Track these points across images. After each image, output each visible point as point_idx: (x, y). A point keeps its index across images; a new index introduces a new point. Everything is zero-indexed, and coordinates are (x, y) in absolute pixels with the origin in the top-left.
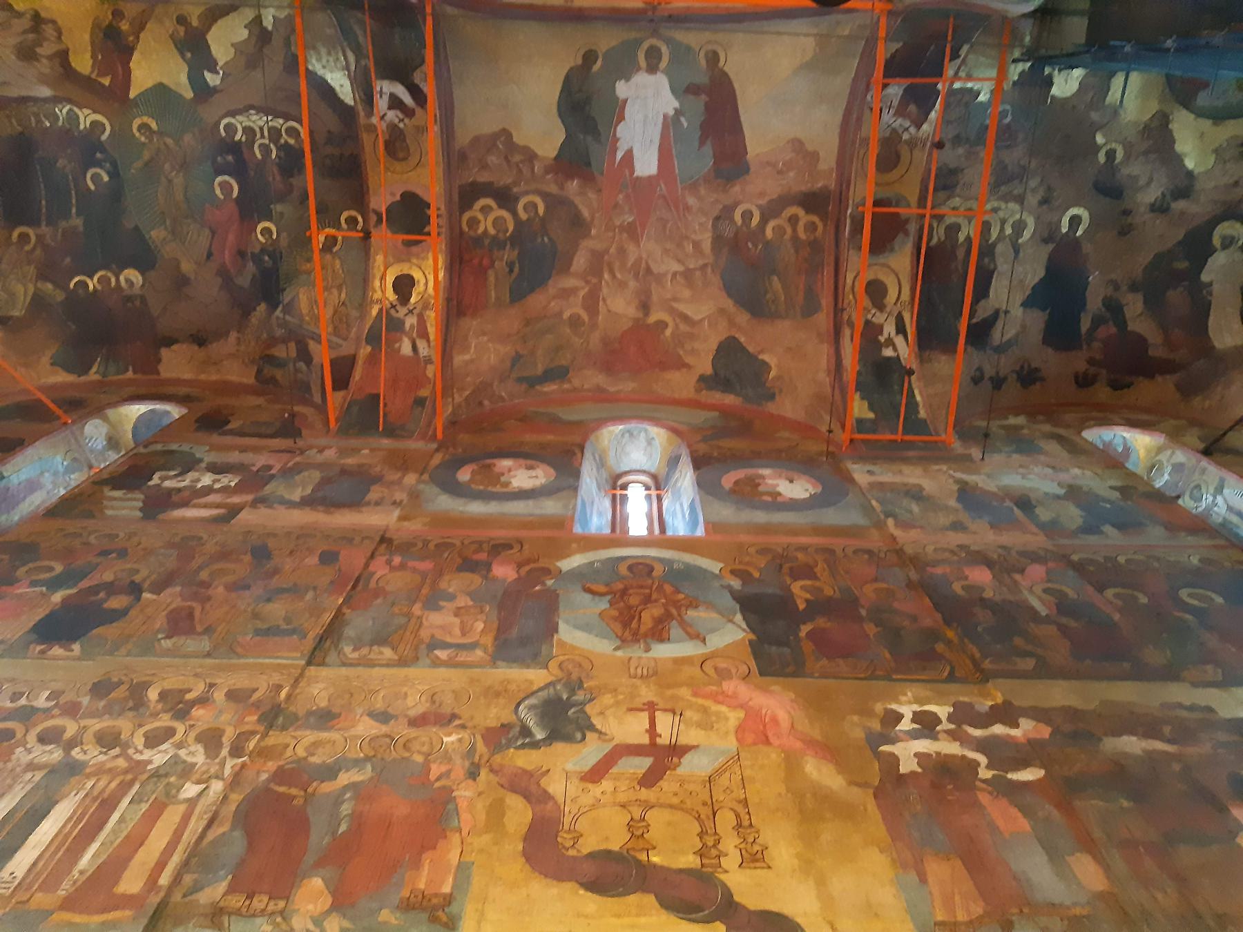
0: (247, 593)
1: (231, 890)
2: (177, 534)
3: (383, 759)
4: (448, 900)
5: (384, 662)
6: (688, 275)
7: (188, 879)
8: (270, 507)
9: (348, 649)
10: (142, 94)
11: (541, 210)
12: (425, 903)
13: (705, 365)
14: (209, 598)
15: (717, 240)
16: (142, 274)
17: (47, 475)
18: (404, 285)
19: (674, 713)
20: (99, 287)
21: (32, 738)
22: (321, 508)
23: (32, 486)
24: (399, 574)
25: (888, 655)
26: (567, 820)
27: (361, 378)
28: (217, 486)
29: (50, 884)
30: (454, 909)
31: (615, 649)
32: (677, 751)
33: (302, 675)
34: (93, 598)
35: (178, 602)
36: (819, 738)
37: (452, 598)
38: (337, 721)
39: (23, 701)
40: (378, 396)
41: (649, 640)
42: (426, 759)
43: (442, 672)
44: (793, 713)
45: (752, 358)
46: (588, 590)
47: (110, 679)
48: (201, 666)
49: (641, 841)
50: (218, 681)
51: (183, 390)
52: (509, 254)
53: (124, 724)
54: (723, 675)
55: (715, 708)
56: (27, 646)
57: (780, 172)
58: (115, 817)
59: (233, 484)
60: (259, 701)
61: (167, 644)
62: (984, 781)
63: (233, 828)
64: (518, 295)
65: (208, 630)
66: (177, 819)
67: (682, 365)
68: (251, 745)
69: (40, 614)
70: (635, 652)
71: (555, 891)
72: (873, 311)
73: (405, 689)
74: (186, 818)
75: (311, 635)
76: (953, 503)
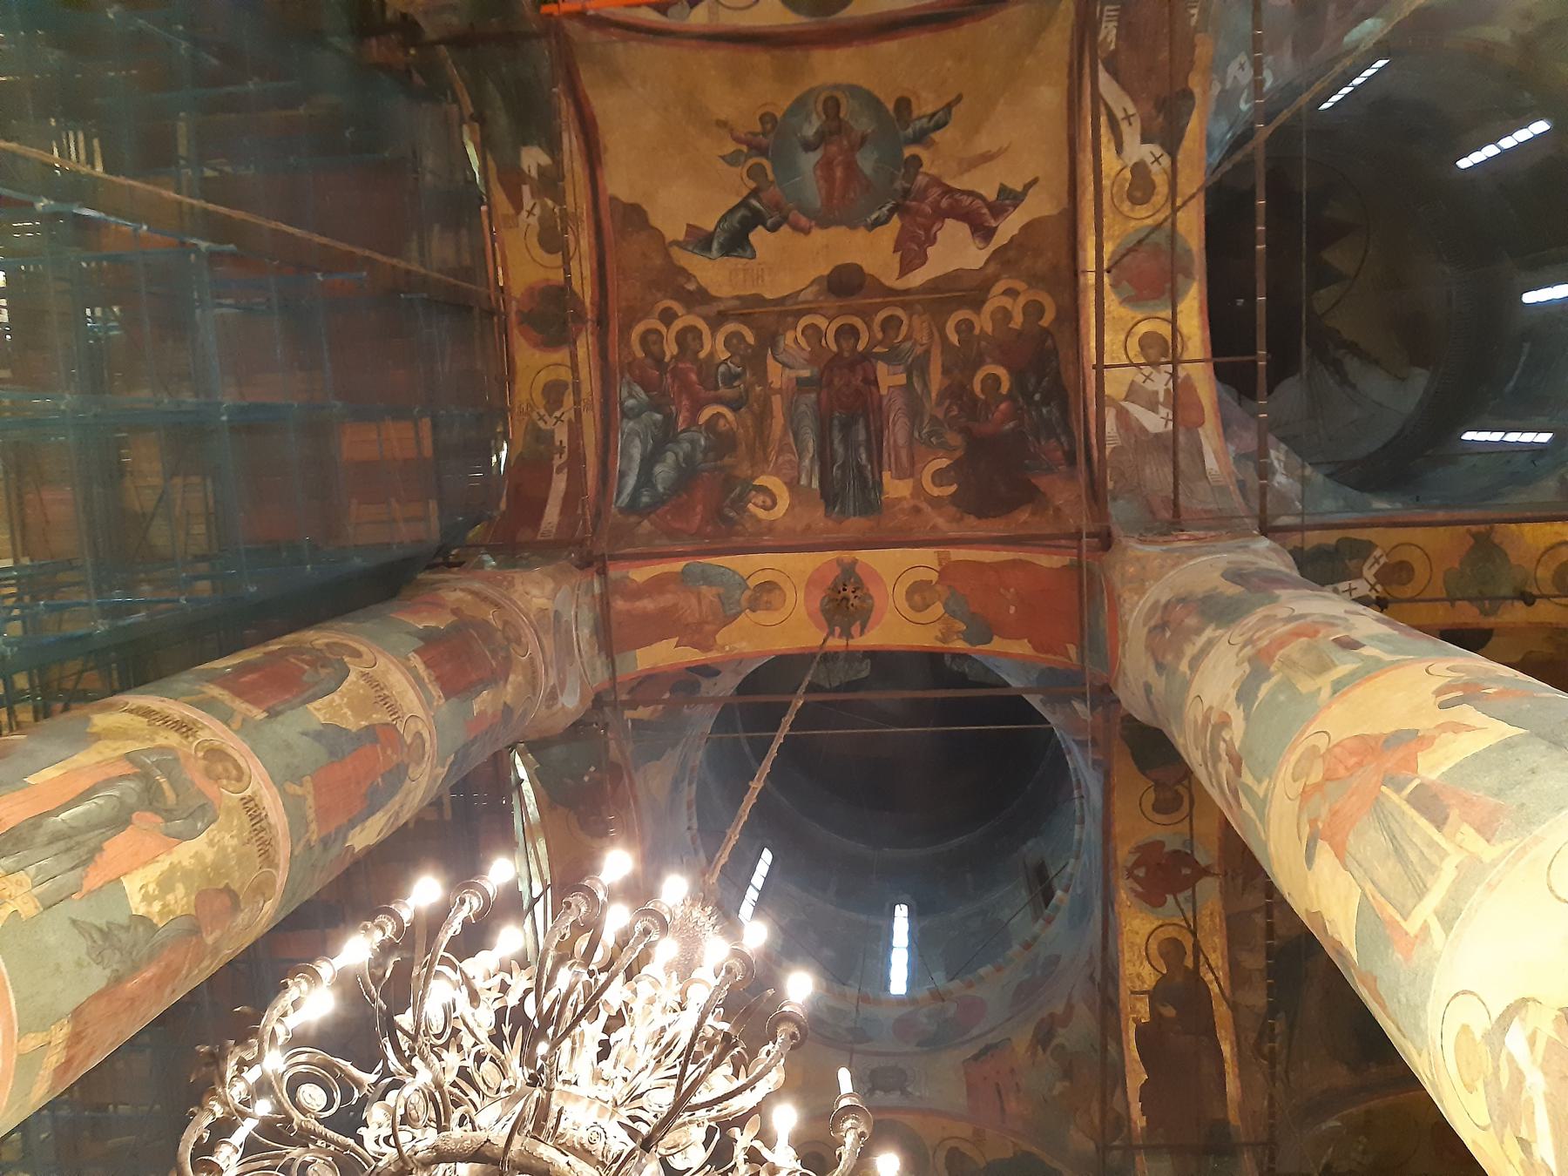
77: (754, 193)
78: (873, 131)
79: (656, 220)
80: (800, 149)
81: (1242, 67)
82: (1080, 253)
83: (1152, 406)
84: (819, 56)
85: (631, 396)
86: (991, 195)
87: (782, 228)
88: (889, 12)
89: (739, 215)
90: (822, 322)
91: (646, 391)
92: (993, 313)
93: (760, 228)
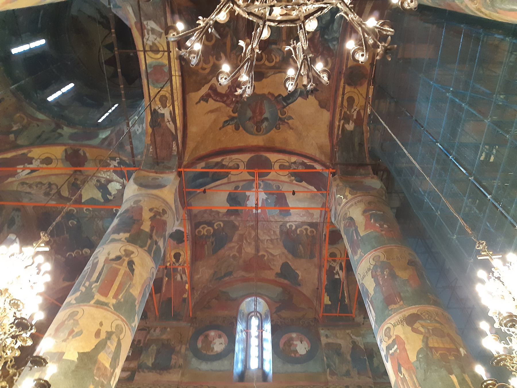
6: (272, 240)
8: (143, 371)
10: (86, 200)
11: (222, 225)
13: (278, 270)
15: (281, 232)
16: (90, 250)
18: (177, 256)
20: (76, 255)
22: (158, 371)
27: (165, 291)
40: (171, 298)
45: (293, 271)
52: (212, 239)
57: (302, 217)
59: (130, 354)
64: (215, 251)
67: (270, 269)
72: (332, 262)
76: (349, 358)
77: (284, 107)
78: (247, 121)
79: (316, 102)
80: (269, 118)
81: (138, 130)
82: (181, 82)
83: (153, 30)
84: (261, 144)
85: (334, 45)
86: (211, 101)
87: (277, 95)
88: (240, 154)
89: (290, 101)
90: (267, 63)
91: (329, 47)
92: (209, 62)
93: (284, 96)
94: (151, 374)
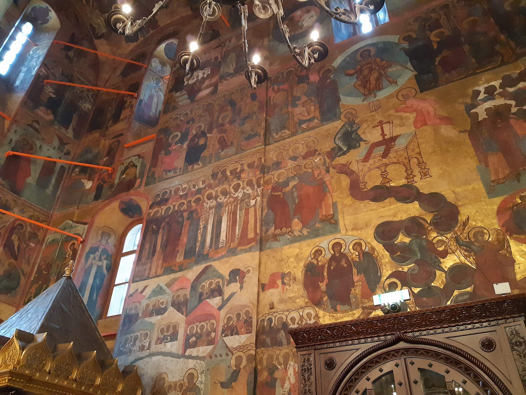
0: (236, 123)
1: (275, 229)
2: (204, 105)
3: (300, 174)
4: (333, 215)
5: (288, 136)
7: (264, 228)
8: (226, 80)
9: (274, 135)
12: (327, 219)
14: (226, 130)
17: (152, 90)
19: (390, 123)
21: (205, 199)
23: (151, 97)
24: (278, 94)
25: (474, 61)
26: (361, 178)
28: (205, 76)
29: (233, 241)
30: (335, 218)
31: (363, 101)
32: (393, 139)
33: (265, 151)
34: (195, 142)
35: (219, 136)
36: (446, 115)
37: (299, 98)
38: (281, 165)
39: (197, 187)
41: (375, 91)
42: (312, 170)
43: (307, 134)
44: (435, 106)
46: (347, 75)
47: (214, 172)
48: (237, 159)
49: (386, 179)
50: (243, 162)
51: (171, 29)
53: (226, 186)
54: (406, 97)
55: (405, 115)
56: (187, 168)
58: (238, 217)
59: (209, 73)
60: (257, 166)
61: (223, 153)
62: (514, 114)
63: (268, 210)
65: (232, 144)
66: (253, 213)
68: (262, 182)
69: (183, 155)
70: (371, 99)
71: (362, 205)
73: (297, 145)
74: (255, 211)
75: (262, 134)
94: (235, 78)
